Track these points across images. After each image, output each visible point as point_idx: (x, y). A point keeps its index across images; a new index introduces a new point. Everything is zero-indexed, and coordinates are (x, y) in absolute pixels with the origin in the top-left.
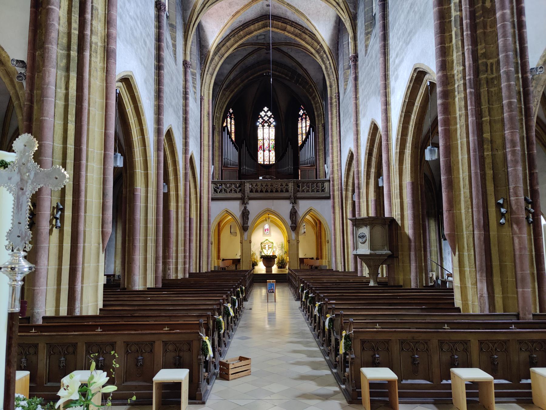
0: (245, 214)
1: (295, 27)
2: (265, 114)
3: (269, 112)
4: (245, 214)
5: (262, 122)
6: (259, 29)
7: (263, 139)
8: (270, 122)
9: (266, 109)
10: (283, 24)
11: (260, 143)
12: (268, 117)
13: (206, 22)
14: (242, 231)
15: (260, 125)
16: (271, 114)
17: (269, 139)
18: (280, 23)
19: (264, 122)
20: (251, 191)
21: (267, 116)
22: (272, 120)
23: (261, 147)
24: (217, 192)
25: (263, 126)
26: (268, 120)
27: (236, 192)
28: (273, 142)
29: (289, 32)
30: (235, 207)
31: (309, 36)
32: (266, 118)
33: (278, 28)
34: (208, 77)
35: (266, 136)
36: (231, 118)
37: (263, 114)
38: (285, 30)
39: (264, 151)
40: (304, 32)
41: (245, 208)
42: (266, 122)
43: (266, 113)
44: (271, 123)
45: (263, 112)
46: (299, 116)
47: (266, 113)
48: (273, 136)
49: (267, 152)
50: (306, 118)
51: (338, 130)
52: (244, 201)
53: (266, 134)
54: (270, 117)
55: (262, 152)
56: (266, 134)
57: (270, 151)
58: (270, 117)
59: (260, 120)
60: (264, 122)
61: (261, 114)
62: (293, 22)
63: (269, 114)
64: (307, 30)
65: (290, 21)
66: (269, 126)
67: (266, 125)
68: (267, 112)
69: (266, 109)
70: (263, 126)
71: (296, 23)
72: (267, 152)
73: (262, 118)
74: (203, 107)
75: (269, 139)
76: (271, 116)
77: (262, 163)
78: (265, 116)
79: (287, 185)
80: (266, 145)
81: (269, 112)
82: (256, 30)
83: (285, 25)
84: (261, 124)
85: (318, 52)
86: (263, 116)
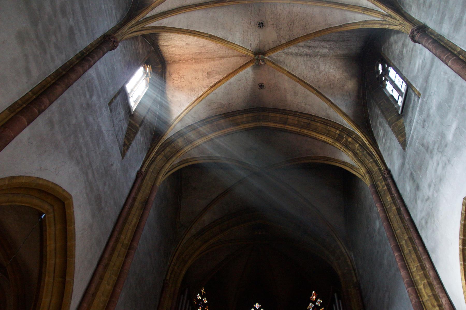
6: (248, 122)
18: (278, 115)
38: (285, 123)
62: (298, 112)
83: (285, 116)
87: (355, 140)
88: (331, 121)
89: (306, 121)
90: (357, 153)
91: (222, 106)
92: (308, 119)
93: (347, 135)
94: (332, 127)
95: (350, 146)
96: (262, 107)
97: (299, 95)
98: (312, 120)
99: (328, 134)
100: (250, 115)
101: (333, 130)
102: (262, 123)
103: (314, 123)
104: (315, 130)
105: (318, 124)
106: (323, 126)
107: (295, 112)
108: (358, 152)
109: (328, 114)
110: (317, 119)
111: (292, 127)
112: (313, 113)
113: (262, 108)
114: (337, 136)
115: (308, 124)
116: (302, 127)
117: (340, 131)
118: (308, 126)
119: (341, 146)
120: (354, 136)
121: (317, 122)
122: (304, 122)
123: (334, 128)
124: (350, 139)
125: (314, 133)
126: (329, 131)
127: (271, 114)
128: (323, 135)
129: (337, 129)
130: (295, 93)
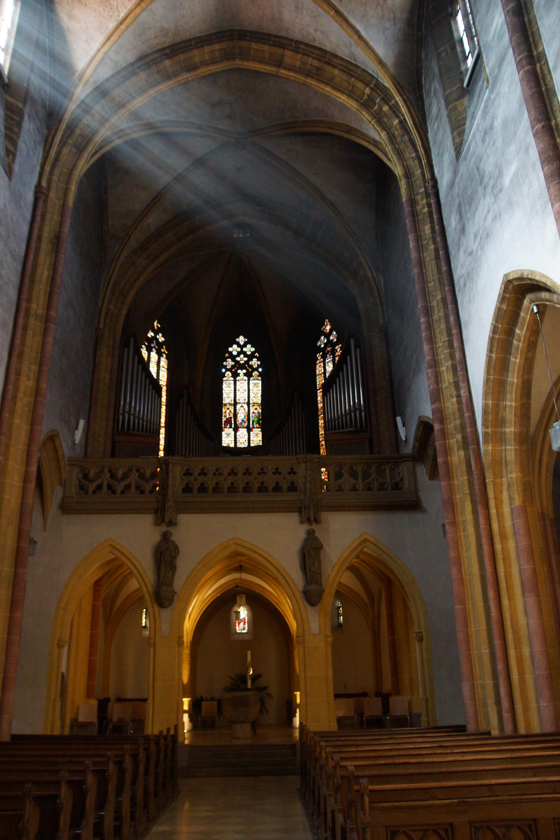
0: (165, 556)
1: (304, 54)
2: (239, 349)
3: (249, 346)
4: (165, 556)
5: (233, 367)
6: (213, 62)
7: (235, 404)
8: (251, 366)
9: (241, 340)
10: (274, 50)
11: (227, 412)
12: (245, 355)
13: (70, 16)
14: (156, 608)
15: (229, 374)
16: (253, 349)
17: (248, 404)
18: (266, 48)
19: (238, 366)
20: (187, 489)
21: (245, 354)
22: (255, 362)
23: (228, 421)
24: (87, 493)
25: (235, 375)
26: (247, 362)
27: (142, 492)
28: (256, 411)
29: (290, 69)
30: (135, 535)
31: (342, 70)
32: (242, 359)
33: (261, 62)
34: (65, 151)
35: (242, 396)
36: (160, 354)
37: (234, 349)
38: (279, 64)
39: (236, 430)
40: (329, 64)
41: (166, 537)
42: (242, 367)
43: (241, 348)
44: (254, 370)
45: (235, 346)
46: (319, 349)
47: (241, 348)
48: (257, 395)
49: (242, 432)
50: (333, 352)
51: (444, 268)
52: (163, 515)
53: (242, 393)
54: (251, 357)
55: (231, 431)
56: (242, 393)
57: (249, 430)
58: (251, 357)
59: (229, 363)
60: (238, 366)
61: (230, 349)
62: (301, 43)
63: (249, 349)
64: (337, 57)
65: (292, 40)
66: (249, 375)
67: (241, 372)
68: (245, 345)
69: (241, 340)
70: (235, 375)
71: (307, 45)
72: (242, 432)
73: (233, 358)
74: (39, 213)
75: (248, 404)
76: (253, 353)
77: (232, 445)
78: (239, 354)
79: (292, 472)
80: (241, 416)
81: (249, 346)
82: (204, 63)
83: (280, 51)
84: (230, 370)
85: (367, 105)
86: (235, 353)
87: (394, 112)
88: (358, 67)
89: (316, 63)
90: (393, 135)
91: (165, 32)
92: (320, 60)
93: (383, 99)
94: (357, 79)
95: (386, 120)
96: (238, 28)
97: (304, 12)
98: (325, 62)
99: (351, 95)
100: (217, 47)
101: (360, 85)
102: (237, 61)
103: (328, 68)
104: (329, 82)
105: (336, 72)
106: (344, 76)
107: (297, 42)
108: (396, 133)
109: (353, 54)
110: (335, 60)
111: (292, 74)
112: (328, 47)
113: (238, 31)
114: (366, 97)
115: (318, 69)
116: (308, 74)
117: (371, 89)
118: (317, 74)
119: (370, 119)
120: (393, 102)
121: (334, 67)
122: (311, 65)
123: (361, 81)
124: (386, 108)
125: (328, 89)
126: (353, 86)
127: (254, 45)
128: (343, 92)
129: (367, 85)
130: (297, 7)
